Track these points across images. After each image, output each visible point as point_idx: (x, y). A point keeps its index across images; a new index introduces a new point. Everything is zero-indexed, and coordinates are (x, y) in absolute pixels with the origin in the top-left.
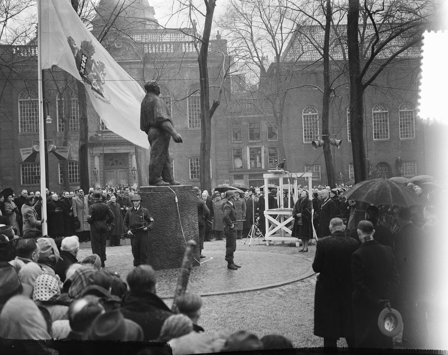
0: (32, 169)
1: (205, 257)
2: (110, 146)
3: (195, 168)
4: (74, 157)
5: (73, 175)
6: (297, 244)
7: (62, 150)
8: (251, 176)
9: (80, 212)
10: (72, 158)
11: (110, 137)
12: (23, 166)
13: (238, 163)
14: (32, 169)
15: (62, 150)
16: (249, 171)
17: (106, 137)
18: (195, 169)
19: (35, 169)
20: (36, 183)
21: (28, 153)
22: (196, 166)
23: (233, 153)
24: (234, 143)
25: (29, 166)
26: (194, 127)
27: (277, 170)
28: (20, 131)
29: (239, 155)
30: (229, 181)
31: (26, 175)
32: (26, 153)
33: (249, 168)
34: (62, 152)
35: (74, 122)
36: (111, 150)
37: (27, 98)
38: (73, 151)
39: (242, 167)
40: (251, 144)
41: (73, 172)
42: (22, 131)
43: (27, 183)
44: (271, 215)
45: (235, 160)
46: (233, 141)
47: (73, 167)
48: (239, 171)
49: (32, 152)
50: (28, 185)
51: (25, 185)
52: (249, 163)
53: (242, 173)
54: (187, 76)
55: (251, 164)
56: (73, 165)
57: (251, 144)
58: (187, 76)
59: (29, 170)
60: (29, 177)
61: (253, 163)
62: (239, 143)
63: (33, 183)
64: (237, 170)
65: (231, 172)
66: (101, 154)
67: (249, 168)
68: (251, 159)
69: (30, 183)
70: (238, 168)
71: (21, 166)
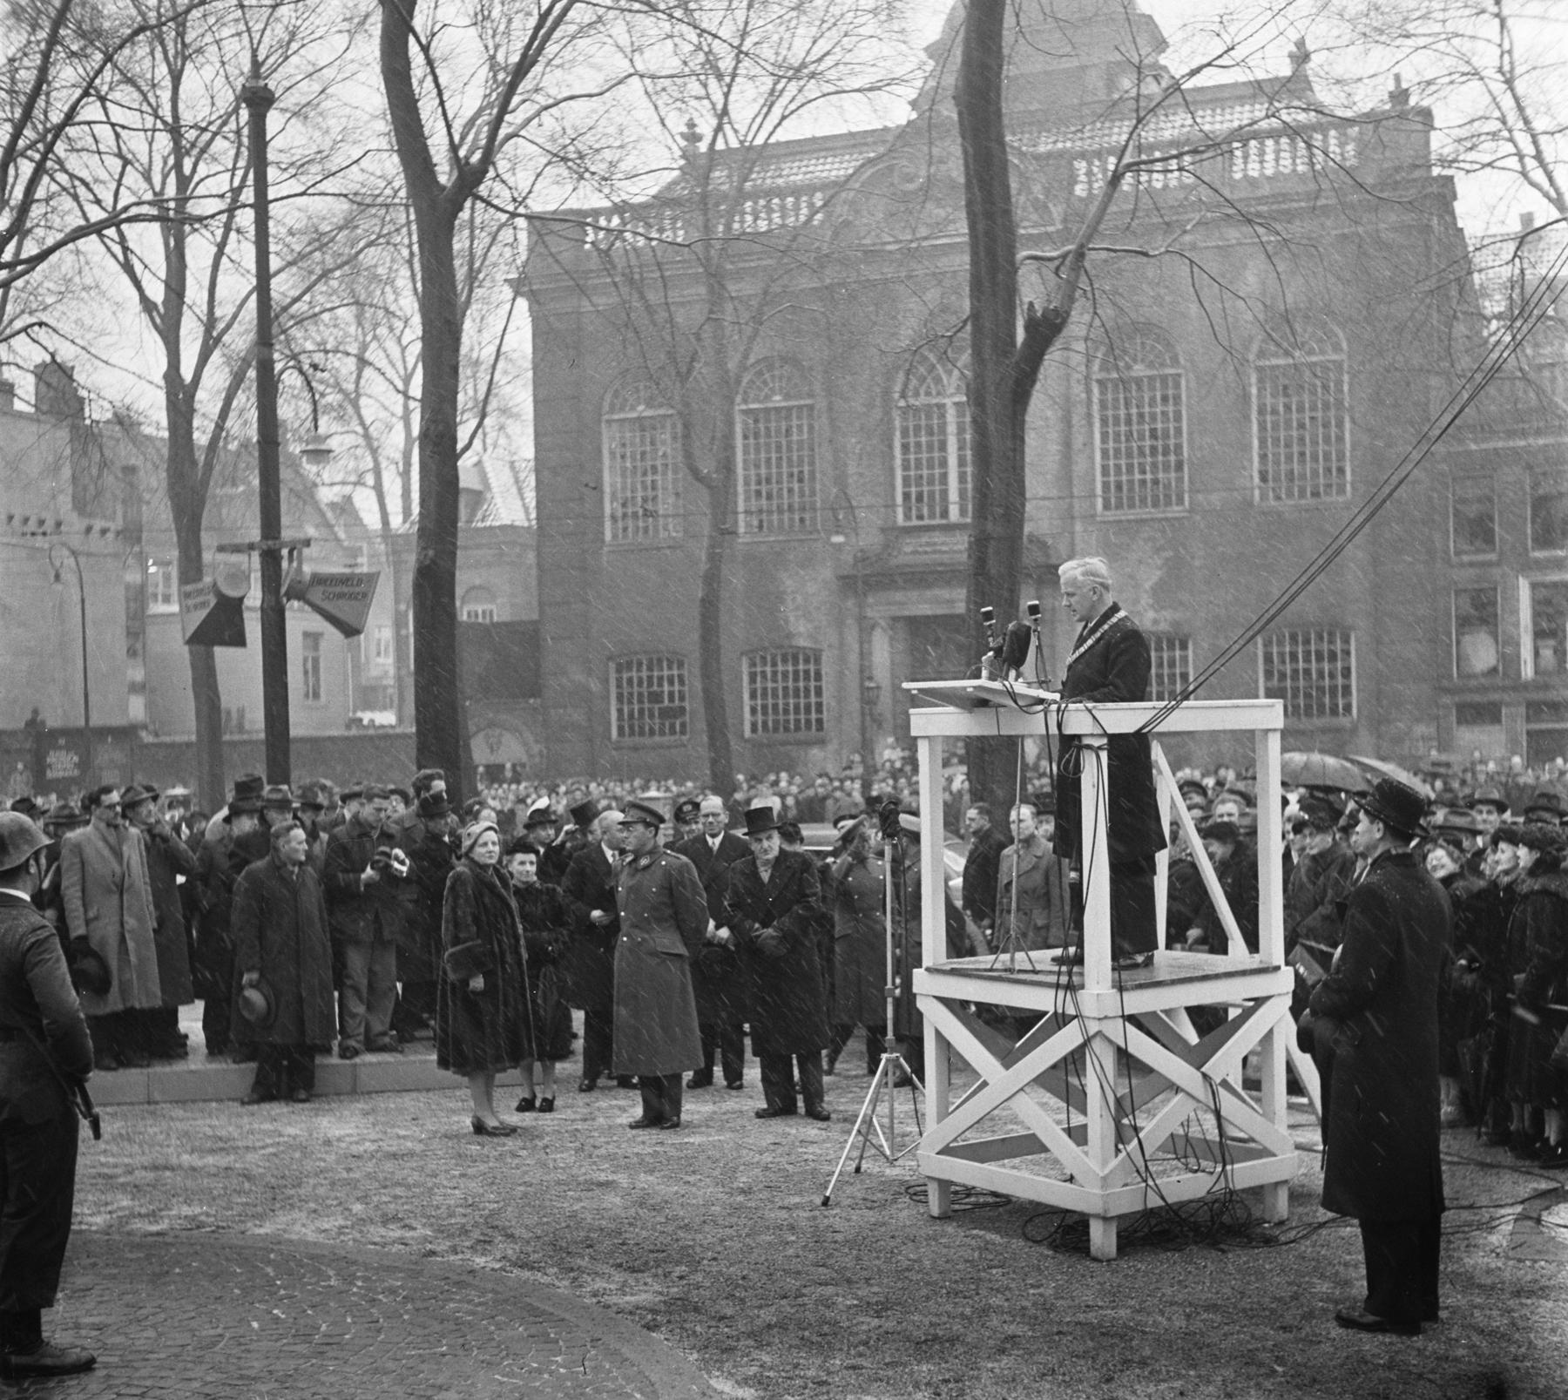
0: (650, 678)
1: (87, 1366)
2: (929, 586)
3: (1283, 676)
4: (800, 634)
5: (797, 707)
6: (1102, 1238)
7: (338, 589)
8: (1535, 710)
9: (107, 907)
10: (789, 636)
11: (935, 552)
12: (619, 671)
13: (1482, 654)
14: (650, 678)
15: (338, 589)
16: (1526, 686)
17: (915, 552)
18: (1283, 676)
19: (661, 679)
20: (662, 733)
21: (203, 604)
22: (1288, 668)
23: (1455, 605)
24: (1462, 565)
25: (639, 670)
26: (1278, 498)
27: (983, 681)
28: (608, 536)
29: (1483, 611)
30: (1432, 730)
31: (630, 702)
32: (196, 607)
33: (1528, 671)
34: (341, 596)
35: (802, 494)
36: (937, 601)
37: (633, 408)
38: (797, 608)
39: (1494, 670)
40: (1540, 565)
41: (797, 690)
42: (615, 536)
43: (632, 733)
44: (946, 1002)
45: (1467, 639)
46: (1457, 553)
47: (796, 673)
48: (1483, 689)
49: (213, 601)
50: (637, 739)
51: (628, 741)
52: (1526, 653)
53: (1495, 697)
54: (1251, 279)
55: (1537, 654)
56: (796, 663)
57: (1540, 565)
58: (1251, 279)
59: (640, 683)
60: (641, 711)
61: (1547, 653)
62: (1483, 564)
63: (652, 732)
64: (1473, 683)
65: (1447, 691)
66: (895, 619)
67: (1528, 671)
68: (1539, 634)
69: (642, 734)
70: (1475, 676)
71: (612, 665)
